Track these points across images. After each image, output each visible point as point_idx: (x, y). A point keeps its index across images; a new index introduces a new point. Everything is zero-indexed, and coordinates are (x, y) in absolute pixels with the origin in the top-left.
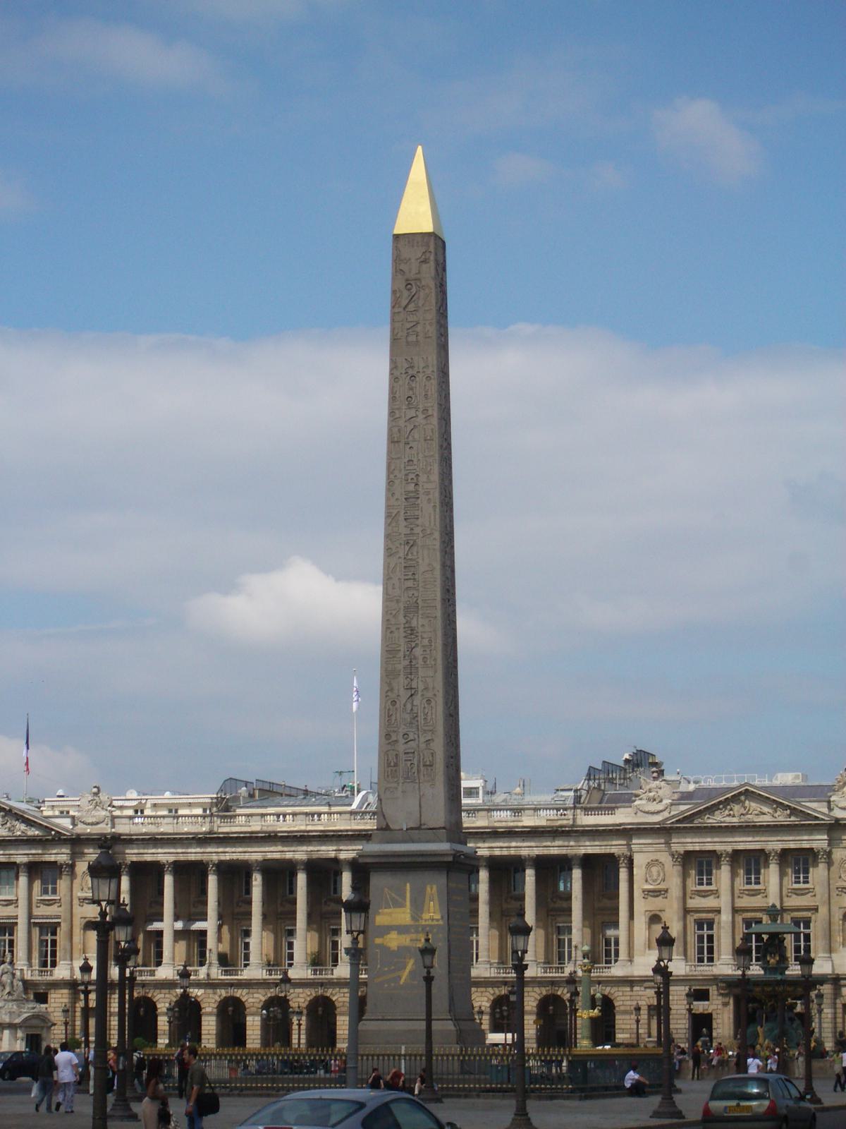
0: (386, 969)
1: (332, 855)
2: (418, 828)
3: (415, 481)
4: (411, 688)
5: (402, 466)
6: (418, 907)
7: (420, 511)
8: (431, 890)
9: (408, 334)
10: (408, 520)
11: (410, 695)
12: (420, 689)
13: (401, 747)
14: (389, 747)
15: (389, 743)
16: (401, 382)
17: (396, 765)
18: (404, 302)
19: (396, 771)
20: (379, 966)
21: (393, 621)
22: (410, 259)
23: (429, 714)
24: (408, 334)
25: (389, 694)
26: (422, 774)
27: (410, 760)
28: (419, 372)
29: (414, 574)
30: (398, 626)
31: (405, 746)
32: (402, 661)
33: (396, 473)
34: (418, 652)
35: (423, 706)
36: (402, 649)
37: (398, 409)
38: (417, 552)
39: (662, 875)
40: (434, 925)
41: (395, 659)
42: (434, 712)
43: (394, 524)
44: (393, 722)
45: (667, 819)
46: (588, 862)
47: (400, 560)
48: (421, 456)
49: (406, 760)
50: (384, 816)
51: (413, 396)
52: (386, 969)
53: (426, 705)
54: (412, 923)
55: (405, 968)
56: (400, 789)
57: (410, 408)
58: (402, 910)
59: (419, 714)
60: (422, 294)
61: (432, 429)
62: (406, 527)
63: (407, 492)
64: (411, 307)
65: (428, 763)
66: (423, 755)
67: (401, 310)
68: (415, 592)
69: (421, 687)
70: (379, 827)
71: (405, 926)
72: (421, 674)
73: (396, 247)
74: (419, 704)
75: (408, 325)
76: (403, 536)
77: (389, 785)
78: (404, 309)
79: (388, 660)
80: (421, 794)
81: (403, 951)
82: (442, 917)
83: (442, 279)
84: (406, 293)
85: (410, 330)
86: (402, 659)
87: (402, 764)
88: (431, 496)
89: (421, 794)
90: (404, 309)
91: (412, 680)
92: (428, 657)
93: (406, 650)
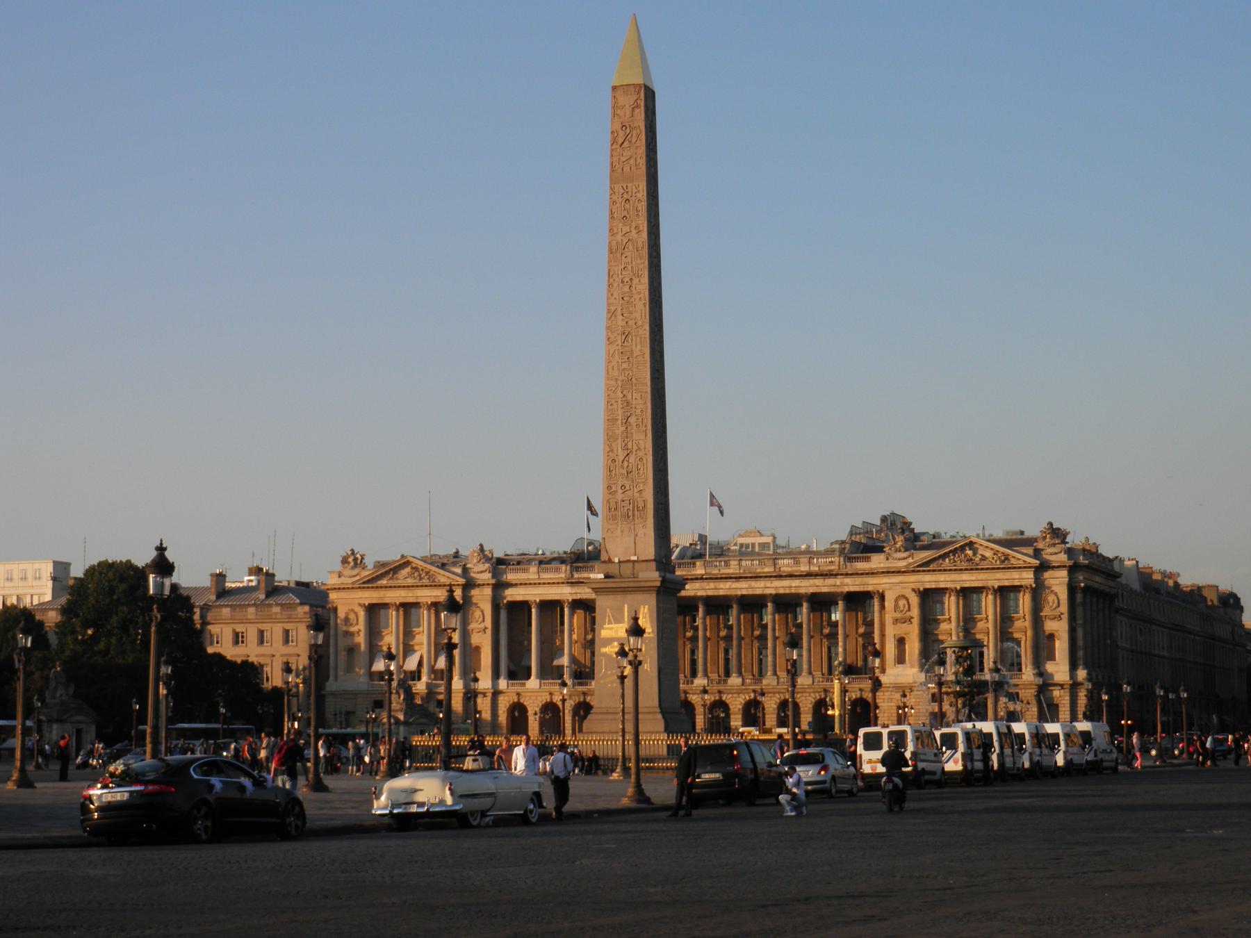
0: (609, 672)
5: (620, 273)
12: (634, 450)
14: (610, 496)
15: (610, 493)
18: (620, 141)
21: (613, 396)
25: (610, 453)
33: (615, 277)
34: (632, 420)
38: (632, 340)
39: (907, 606)
43: (613, 318)
45: (910, 564)
47: (618, 347)
48: (634, 263)
51: (628, 216)
56: (619, 530)
57: (626, 225)
60: (634, 133)
61: (643, 242)
66: (637, 502)
67: (618, 146)
69: (635, 448)
72: (635, 436)
73: (614, 97)
75: (623, 159)
77: (610, 527)
78: (621, 146)
82: (653, 631)
83: (652, 121)
90: (621, 146)
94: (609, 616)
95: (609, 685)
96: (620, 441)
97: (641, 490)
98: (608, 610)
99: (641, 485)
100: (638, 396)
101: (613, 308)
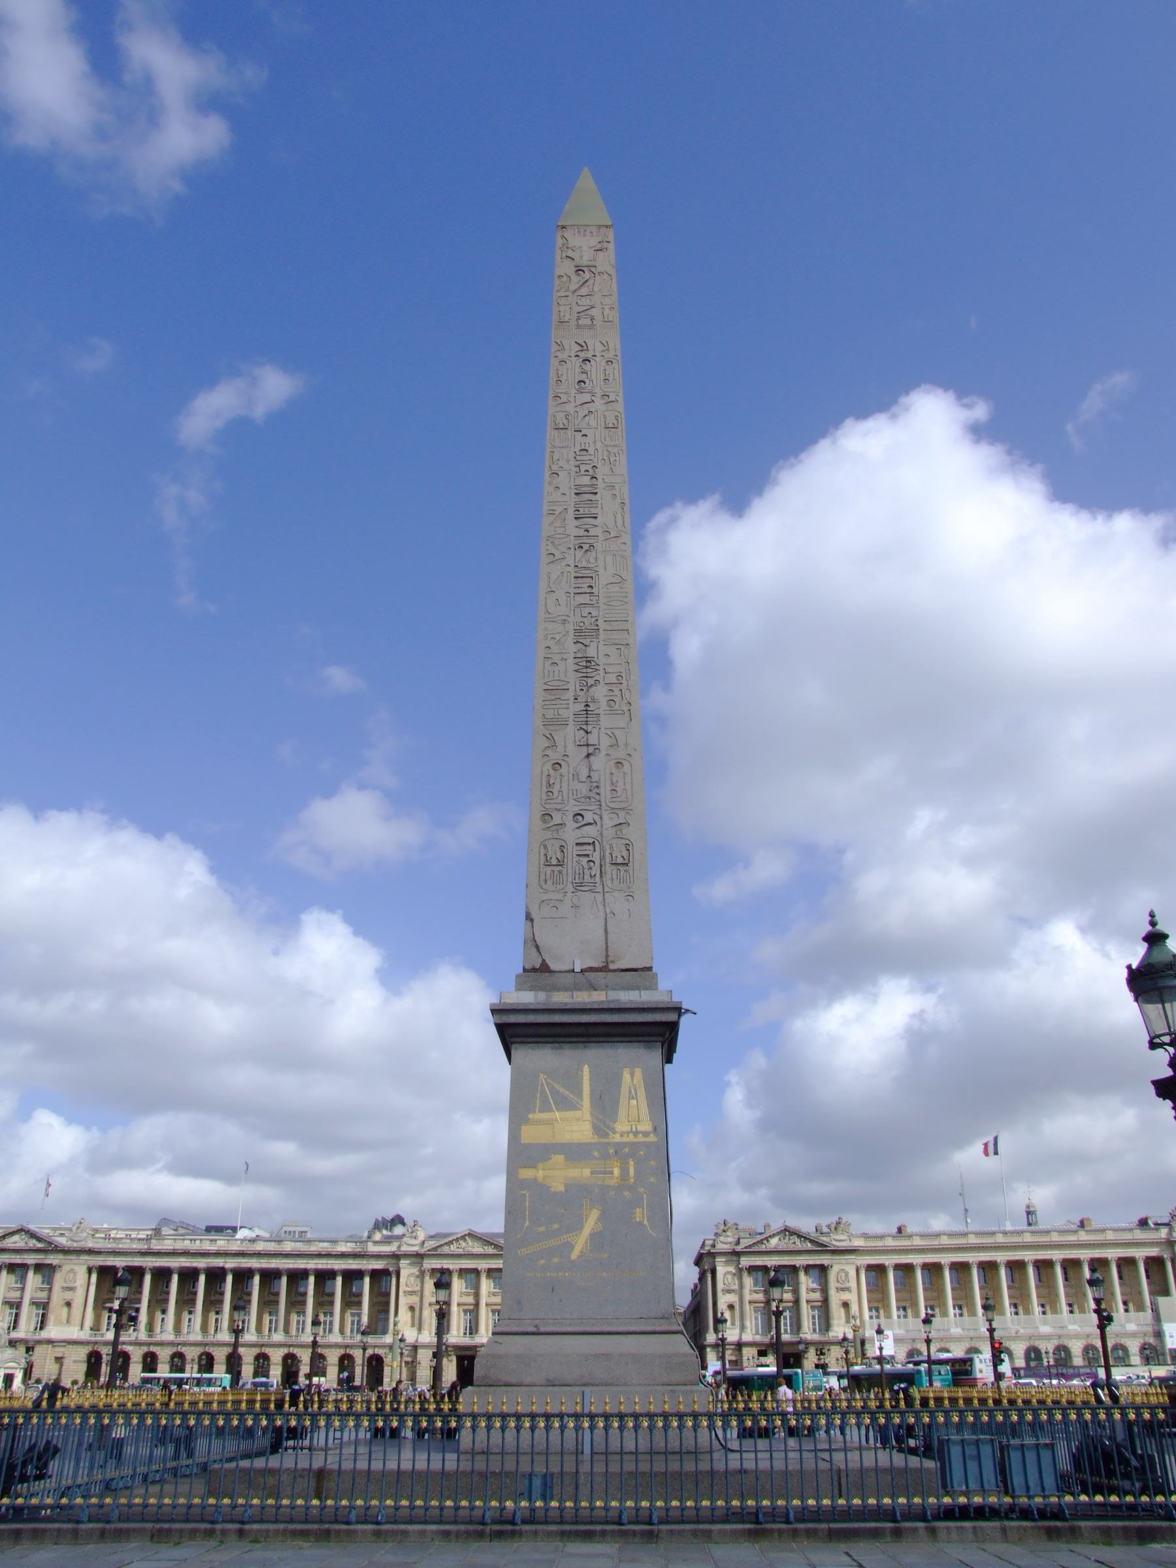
0: (542, 1229)
1: (221, 1265)
2: (604, 969)
3: (591, 472)
4: (588, 745)
8: (632, 1079)
9: (578, 319)
10: (579, 520)
11: (585, 754)
13: (571, 834)
14: (548, 834)
15: (544, 829)
16: (569, 365)
17: (560, 864)
18: (573, 287)
19: (560, 872)
20: (527, 1223)
21: (555, 649)
22: (581, 247)
23: (620, 783)
24: (578, 319)
25: (548, 752)
26: (609, 876)
27: (588, 855)
28: (595, 356)
29: (591, 587)
30: (565, 656)
31: (579, 833)
32: (571, 706)
34: (600, 692)
35: (608, 772)
36: (572, 688)
37: (566, 393)
38: (596, 559)
40: (639, 1143)
41: (559, 702)
46: (376, 1275)
47: (568, 569)
48: (599, 445)
49: (577, 855)
50: (537, 947)
51: (587, 382)
52: (542, 1229)
53: (614, 770)
54: (596, 1139)
55: (582, 1228)
58: (578, 1113)
61: (616, 417)
62: (577, 527)
64: (584, 291)
65: (620, 860)
66: (611, 848)
69: (605, 742)
70: (528, 967)
71: (580, 1145)
72: (605, 721)
75: (580, 309)
76: (572, 538)
77: (546, 897)
79: (546, 703)
80: (608, 911)
81: (577, 1195)
82: (655, 1129)
84: (575, 278)
85: (583, 314)
87: (573, 863)
88: (616, 492)
91: (587, 733)
92: (617, 699)
93: (578, 690)
94: (543, 1091)
95: (542, 1262)
96: (571, 729)
97: (621, 824)
98: (542, 1077)
99: (622, 814)
100: (612, 651)
101: (559, 509)
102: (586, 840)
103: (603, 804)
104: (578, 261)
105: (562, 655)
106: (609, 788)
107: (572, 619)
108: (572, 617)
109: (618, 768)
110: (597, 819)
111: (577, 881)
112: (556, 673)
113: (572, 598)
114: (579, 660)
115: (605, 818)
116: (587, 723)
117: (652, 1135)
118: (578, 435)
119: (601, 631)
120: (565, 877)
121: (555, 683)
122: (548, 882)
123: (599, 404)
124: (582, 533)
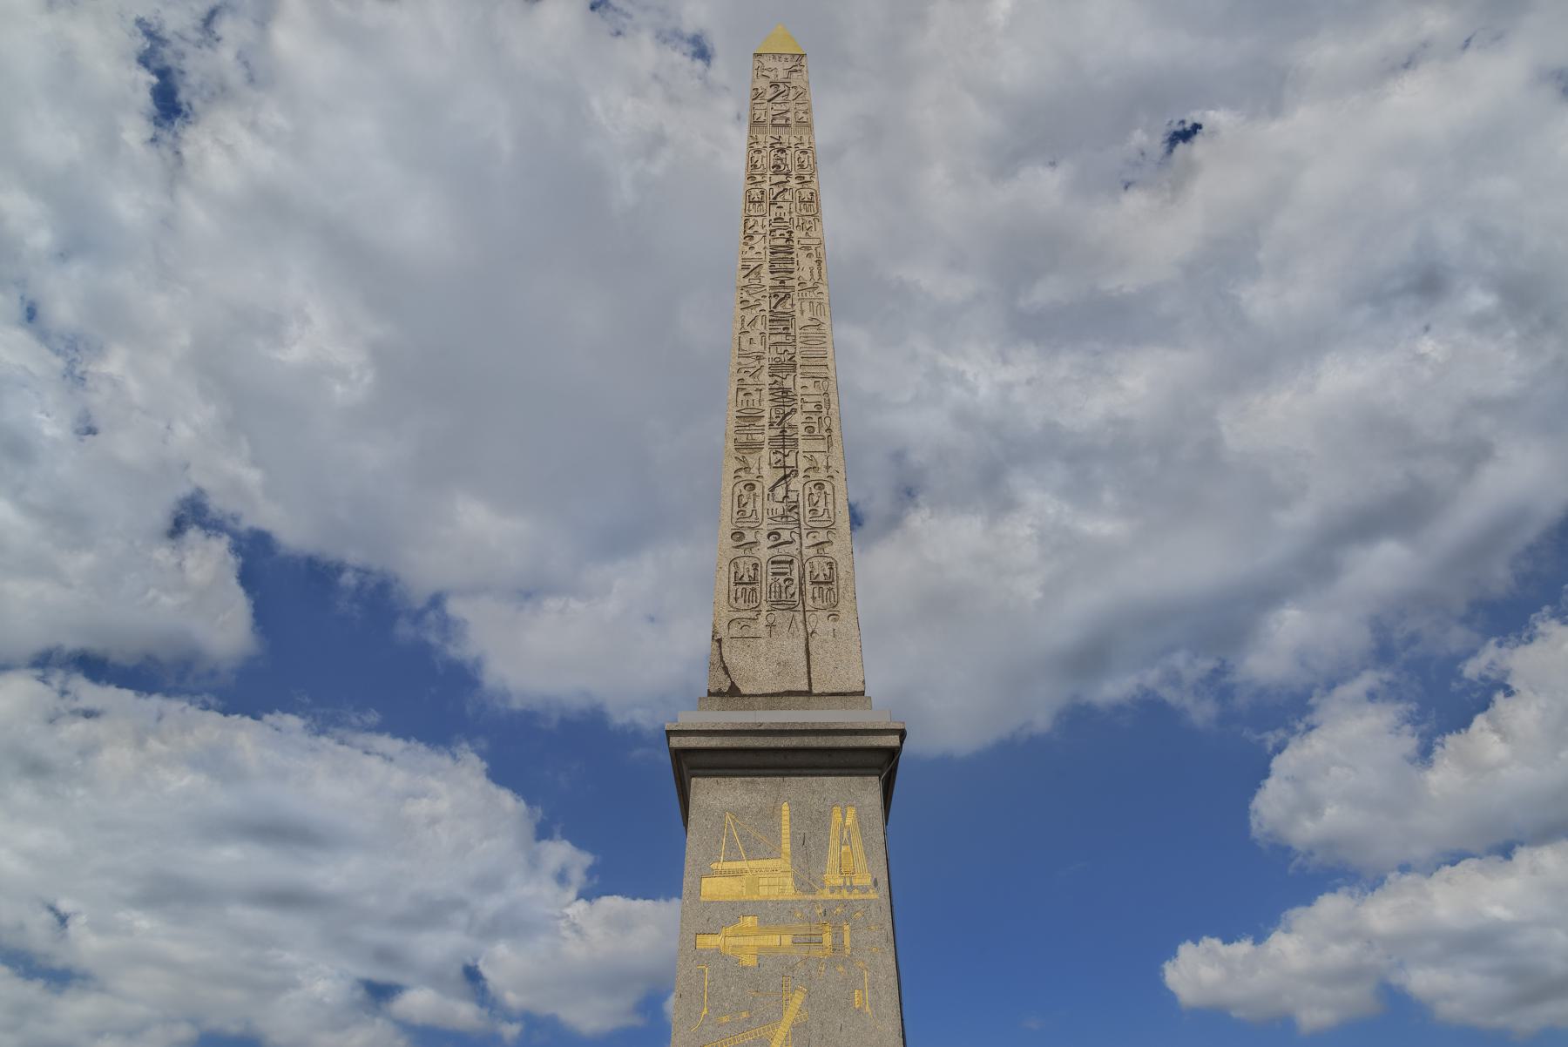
4: (785, 467)
6: (809, 852)
7: (796, 264)
9: (773, 119)
14: (740, 552)
15: (737, 547)
17: (753, 581)
18: (768, 97)
20: (705, 1012)
23: (821, 503)
24: (773, 119)
25: (742, 473)
26: (809, 595)
27: (785, 574)
34: (797, 419)
35: (807, 492)
38: (792, 305)
40: (856, 900)
41: (754, 428)
42: (830, 498)
43: (753, 276)
44: (748, 515)
47: (762, 313)
48: (794, 215)
49: (774, 574)
50: (725, 669)
56: (762, 619)
59: (801, 504)
63: (773, 247)
65: (821, 578)
68: (788, 348)
69: (803, 464)
72: (802, 446)
74: (801, 490)
76: (768, 288)
77: (737, 615)
79: (740, 428)
80: (810, 631)
82: (875, 883)
86: (767, 428)
89: (810, 631)
92: (816, 426)
96: (765, 452)
97: (822, 543)
98: (728, 817)
102: (783, 558)
103: (802, 523)
104: (773, 78)
105: (757, 387)
106: (808, 508)
107: (767, 355)
108: (768, 354)
109: (820, 489)
110: (796, 537)
111: (773, 599)
112: (750, 402)
113: (767, 337)
114: (775, 391)
115: (804, 536)
116: (784, 447)
117: (871, 891)
118: (774, 208)
119: (798, 366)
120: (758, 595)
121: (748, 411)
122: (739, 601)
123: (793, 182)
124: (777, 283)
